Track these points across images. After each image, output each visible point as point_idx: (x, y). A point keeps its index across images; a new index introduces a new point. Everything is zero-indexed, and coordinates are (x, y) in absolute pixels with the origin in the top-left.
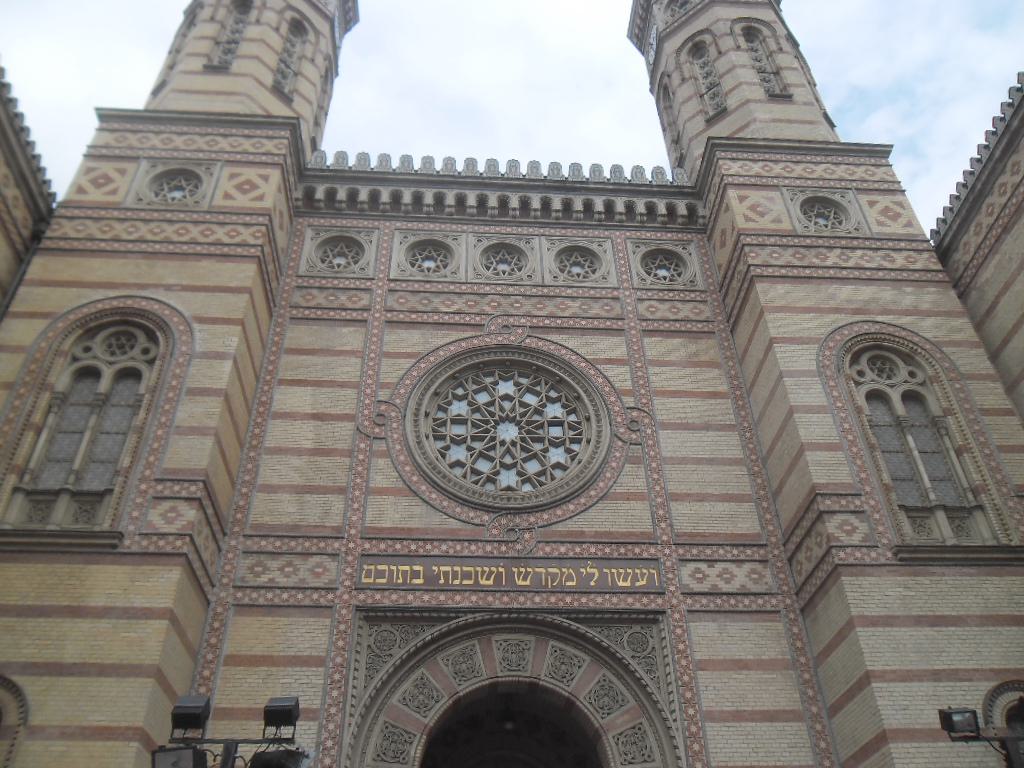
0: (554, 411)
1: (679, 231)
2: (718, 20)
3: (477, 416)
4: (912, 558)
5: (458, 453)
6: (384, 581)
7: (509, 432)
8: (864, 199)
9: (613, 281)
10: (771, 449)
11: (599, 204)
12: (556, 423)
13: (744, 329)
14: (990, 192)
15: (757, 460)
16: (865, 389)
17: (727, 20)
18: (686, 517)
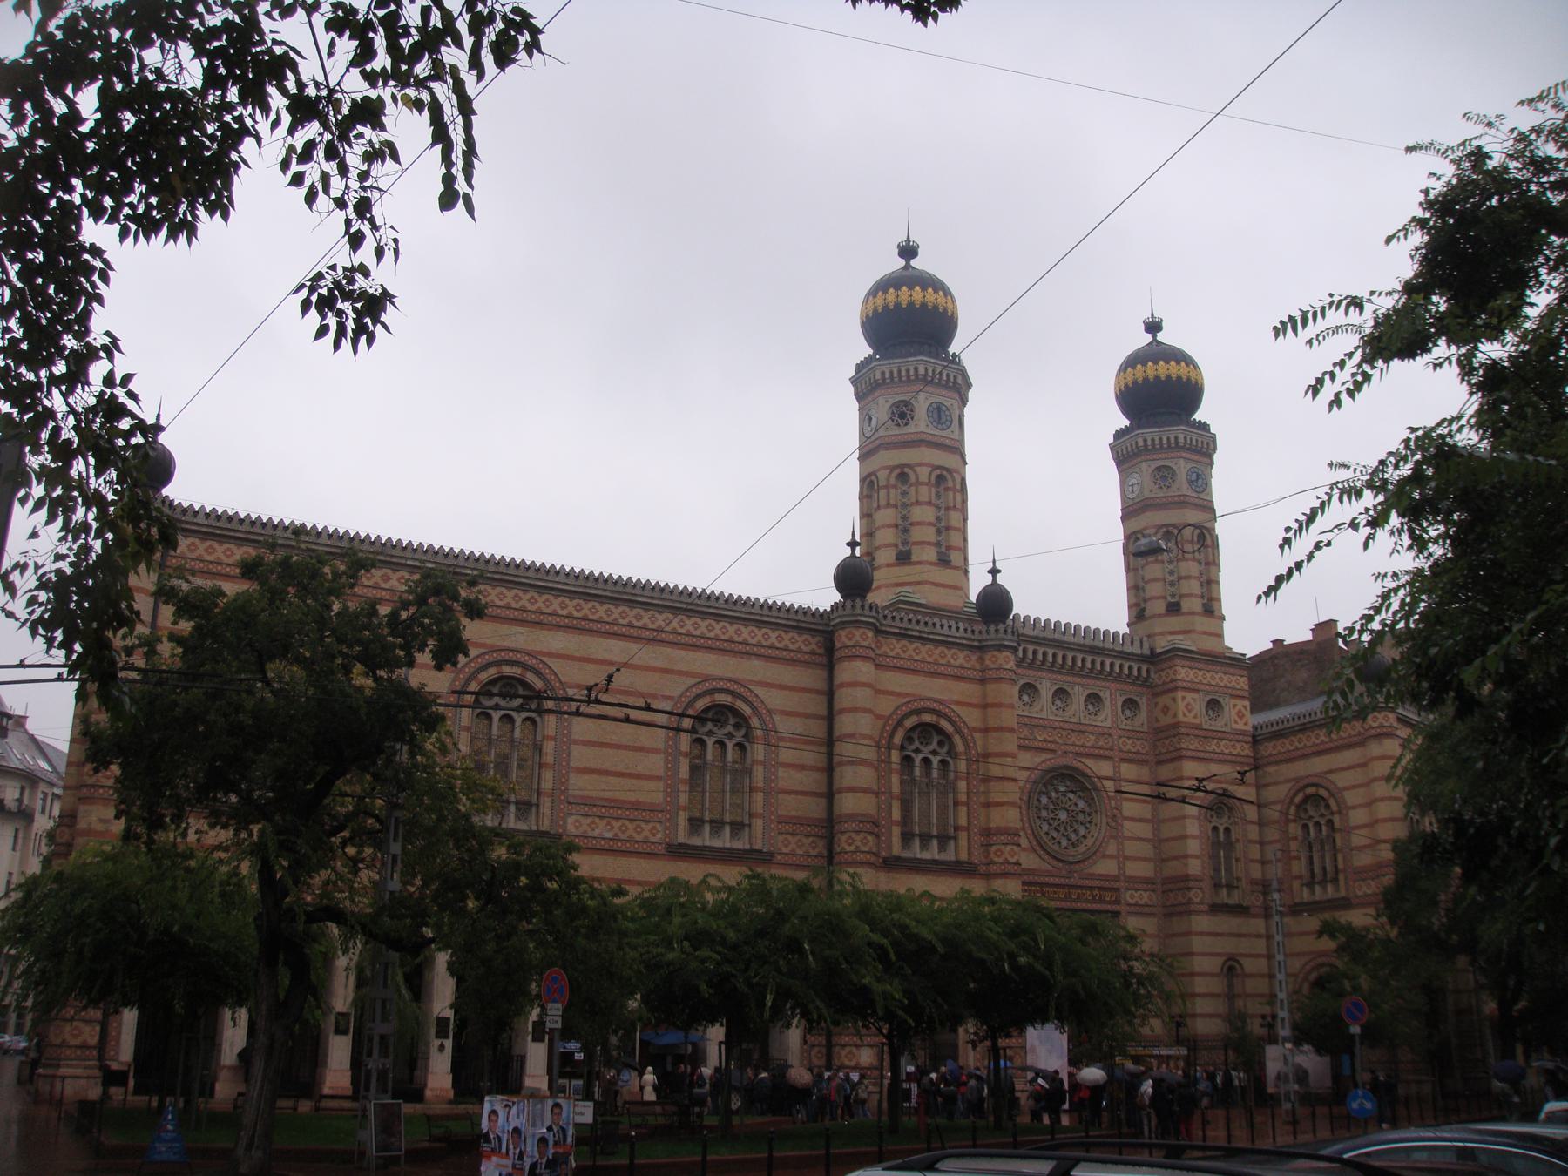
0: (1081, 804)
3: (1051, 806)
4: (1216, 909)
5: (1045, 827)
7: (1063, 816)
8: (1233, 701)
9: (1108, 723)
10: (1167, 840)
11: (1108, 662)
12: (1083, 812)
15: (1158, 841)
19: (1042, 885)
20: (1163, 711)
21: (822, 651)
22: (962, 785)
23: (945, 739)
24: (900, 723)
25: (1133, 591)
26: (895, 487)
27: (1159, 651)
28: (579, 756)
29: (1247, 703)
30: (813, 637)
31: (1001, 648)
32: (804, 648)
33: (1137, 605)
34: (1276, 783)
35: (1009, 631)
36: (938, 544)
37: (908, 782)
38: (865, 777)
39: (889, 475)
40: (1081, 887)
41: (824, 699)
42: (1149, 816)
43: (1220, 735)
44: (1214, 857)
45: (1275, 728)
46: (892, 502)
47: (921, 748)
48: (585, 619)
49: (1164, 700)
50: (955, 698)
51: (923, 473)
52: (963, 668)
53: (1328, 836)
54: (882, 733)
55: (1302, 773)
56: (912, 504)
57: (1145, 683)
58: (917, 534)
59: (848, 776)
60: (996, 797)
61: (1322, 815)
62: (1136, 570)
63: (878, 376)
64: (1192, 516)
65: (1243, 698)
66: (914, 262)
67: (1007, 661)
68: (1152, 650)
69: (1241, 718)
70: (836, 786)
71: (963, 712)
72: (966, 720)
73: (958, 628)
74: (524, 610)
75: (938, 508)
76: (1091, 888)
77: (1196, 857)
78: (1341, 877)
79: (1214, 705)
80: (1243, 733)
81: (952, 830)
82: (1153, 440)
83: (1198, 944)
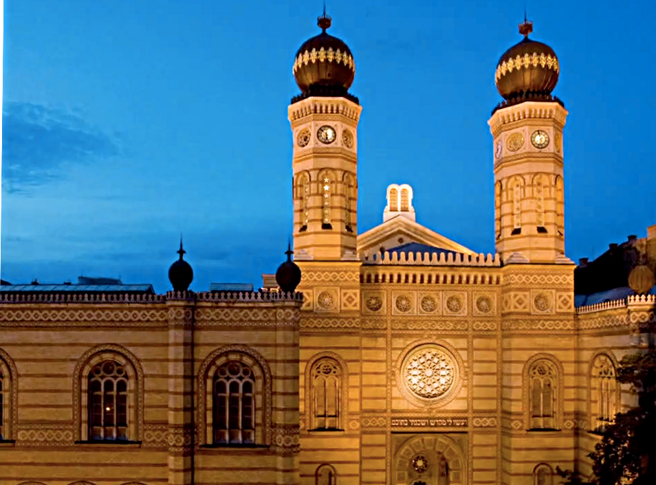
6: (397, 424)
18: (478, 405)
19: (408, 418)
22: (259, 398)
24: (213, 363)
28: (23, 398)
40: (438, 418)
47: (231, 376)
71: (261, 350)
76: (446, 419)
81: (253, 425)
83: (515, 456)
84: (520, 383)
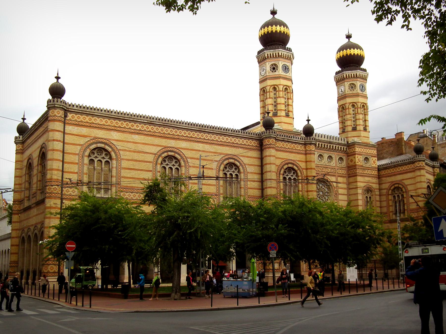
0: (326, 190)
1: (344, 153)
2: (359, 102)
3: (318, 191)
7: (321, 193)
8: (372, 158)
9: (334, 165)
11: (334, 146)
13: (351, 179)
14: (389, 169)
16: (366, 196)
17: (361, 102)
20: (351, 161)
21: (258, 146)
23: (295, 172)
24: (282, 167)
25: (341, 124)
26: (272, 92)
27: (349, 142)
29: (376, 158)
30: (256, 141)
31: (311, 144)
32: (254, 145)
33: (342, 128)
34: (385, 183)
35: (314, 139)
36: (285, 110)
37: (285, 185)
38: (274, 184)
39: (270, 87)
41: (260, 160)
42: (346, 193)
43: (368, 169)
44: (366, 205)
45: (385, 166)
46: (271, 97)
47: (288, 174)
48: (191, 137)
49: (351, 158)
50: (298, 159)
51: (281, 87)
52: (300, 150)
53: (402, 199)
54: (277, 171)
55: (394, 180)
56: (277, 98)
57: (346, 152)
58: (279, 107)
59: (268, 184)
60: (310, 189)
61: (400, 193)
62: (342, 117)
63: (266, 56)
64: (361, 100)
65: (375, 157)
66: (276, 16)
67: (312, 148)
68: (348, 142)
69: (374, 163)
70: (264, 187)
71: (300, 163)
72: (301, 166)
73: (298, 138)
74: (173, 135)
75: (285, 99)
77: (361, 206)
78: (406, 212)
79: (366, 159)
80: (375, 168)
82: (349, 75)
84: (361, 198)
